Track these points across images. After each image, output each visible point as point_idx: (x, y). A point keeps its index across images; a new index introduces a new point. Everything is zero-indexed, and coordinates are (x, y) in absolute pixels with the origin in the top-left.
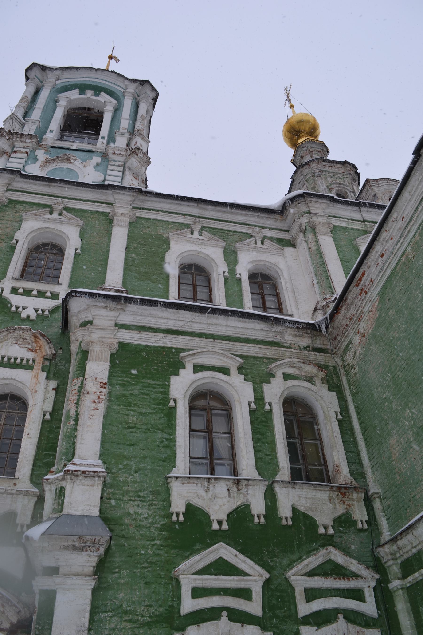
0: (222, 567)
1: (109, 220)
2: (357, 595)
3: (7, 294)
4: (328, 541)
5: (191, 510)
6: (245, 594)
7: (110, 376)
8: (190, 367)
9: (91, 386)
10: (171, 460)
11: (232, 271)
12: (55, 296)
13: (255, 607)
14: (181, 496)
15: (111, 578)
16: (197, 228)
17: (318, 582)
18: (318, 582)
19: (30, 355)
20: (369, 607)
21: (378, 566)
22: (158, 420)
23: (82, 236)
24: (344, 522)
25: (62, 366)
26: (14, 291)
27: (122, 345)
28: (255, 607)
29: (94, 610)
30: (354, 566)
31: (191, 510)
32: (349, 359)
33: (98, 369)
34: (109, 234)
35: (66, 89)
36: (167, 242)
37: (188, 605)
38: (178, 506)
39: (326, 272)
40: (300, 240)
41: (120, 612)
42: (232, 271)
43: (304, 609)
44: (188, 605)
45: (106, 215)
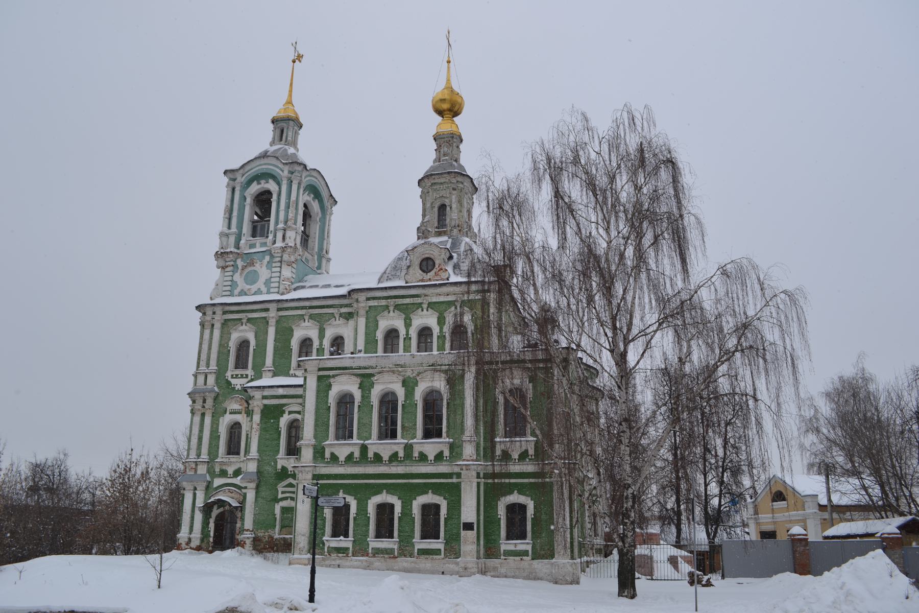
0: (291, 485)
1: (266, 321)
3: (230, 379)
5: (283, 468)
7: (261, 420)
8: (287, 413)
9: (255, 426)
10: (278, 451)
11: (321, 344)
12: (247, 375)
15: (261, 489)
16: (306, 318)
19: (240, 407)
22: (275, 436)
23: (256, 337)
25: (249, 413)
26: (232, 377)
27: (265, 405)
29: (256, 498)
31: (283, 468)
33: (257, 418)
35: (249, 183)
36: (292, 331)
37: (280, 496)
38: (279, 467)
41: (263, 498)
42: (321, 344)
44: (280, 496)
45: (265, 318)
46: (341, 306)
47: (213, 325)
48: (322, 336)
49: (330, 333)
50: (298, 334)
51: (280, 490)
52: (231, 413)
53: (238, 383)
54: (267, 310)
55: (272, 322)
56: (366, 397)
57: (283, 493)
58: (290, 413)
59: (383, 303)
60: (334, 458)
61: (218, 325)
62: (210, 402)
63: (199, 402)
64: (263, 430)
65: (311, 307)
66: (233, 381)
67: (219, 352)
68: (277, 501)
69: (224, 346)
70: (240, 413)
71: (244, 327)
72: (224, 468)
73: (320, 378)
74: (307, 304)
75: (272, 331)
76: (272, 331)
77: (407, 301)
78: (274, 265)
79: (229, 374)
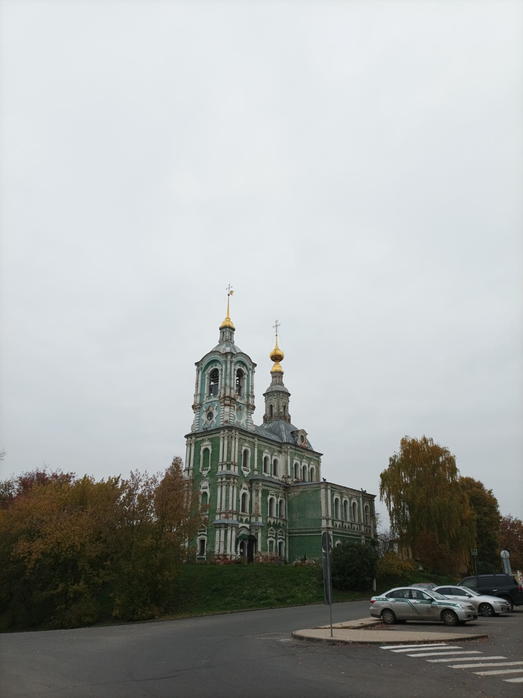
0: (271, 530)
2: (283, 536)
4: (281, 527)
6: (273, 534)
13: (274, 536)
14: (269, 519)
17: (280, 533)
18: (280, 533)
20: (284, 538)
21: (286, 532)
24: (283, 524)
28: (274, 536)
30: (284, 532)
32: (289, 495)
33: (260, 495)
34: (254, 450)
36: (262, 452)
37: (269, 535)
39: (287, 468)
40: (283, 454)
43: (279, 537)
46: (276, 446)
47: (235, 438)
48: (271, 459)
49: (274, 458)
50: (264, 455)
51: (269, 532)
52: (244, 489)
53: (246, 473)
54: (254, 438)
55: (256, 446)
56: (341, 502)
57: (270, 534)
58: (271, 495)
59: (294, 451)
60: (336, 525)
61: (237, 440)
62: (236, 481)
63: (232, 480)
64: (262, 501)
65: (267, 443)
66: (245, 472)
67: (238, 455)
68: (267, 537)
69: (240, 452)
70: (246, 489)
71: (246, 444)
72: (242, 517)
73: (332, 491)
74: (267, 441)
75: (256, 450)
76: (256, 450)
77: (300, 453)
78: (249, 414)
79: (242, 467)
